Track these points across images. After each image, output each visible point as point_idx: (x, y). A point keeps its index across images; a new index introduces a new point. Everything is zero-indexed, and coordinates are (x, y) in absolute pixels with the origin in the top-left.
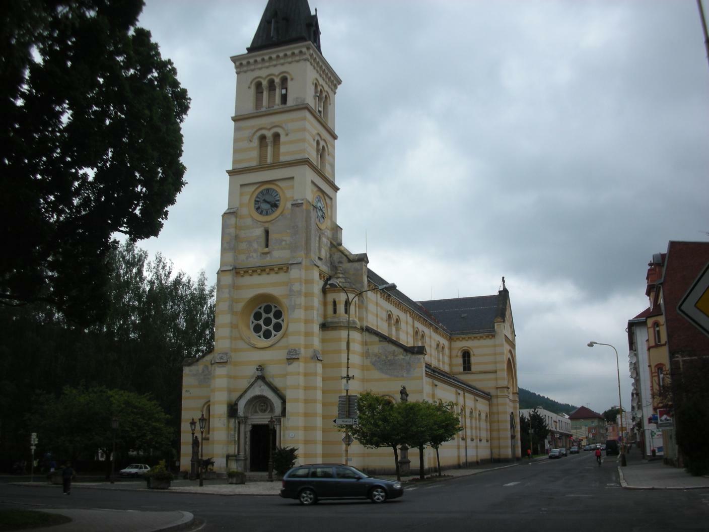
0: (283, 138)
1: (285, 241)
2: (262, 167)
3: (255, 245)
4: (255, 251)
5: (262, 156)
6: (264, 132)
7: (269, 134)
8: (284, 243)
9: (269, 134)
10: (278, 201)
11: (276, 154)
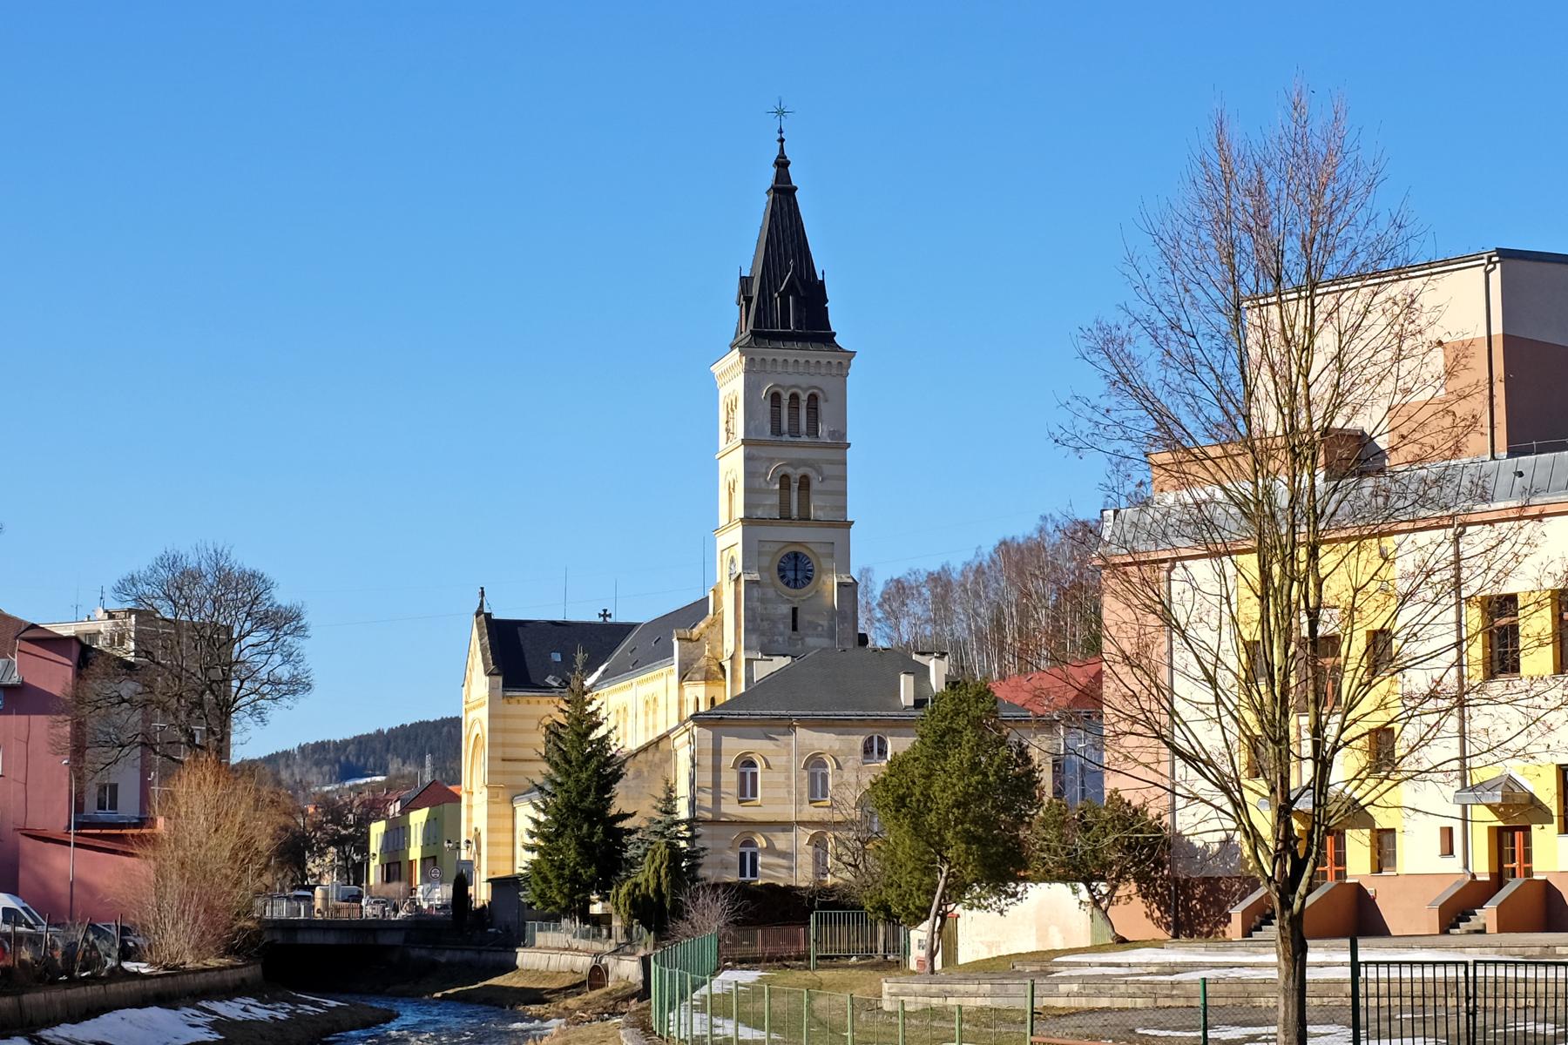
0: (815, 485)
1: (822, 626)
2: (785, 517)
3: (781, 627)
4: (781, 634)
5: (784, 505)
6: (789, 470)
7: (796, 474)
8: (820, 629)
9: (796, 474)
10: (811, 571)
11: (804, 504)
